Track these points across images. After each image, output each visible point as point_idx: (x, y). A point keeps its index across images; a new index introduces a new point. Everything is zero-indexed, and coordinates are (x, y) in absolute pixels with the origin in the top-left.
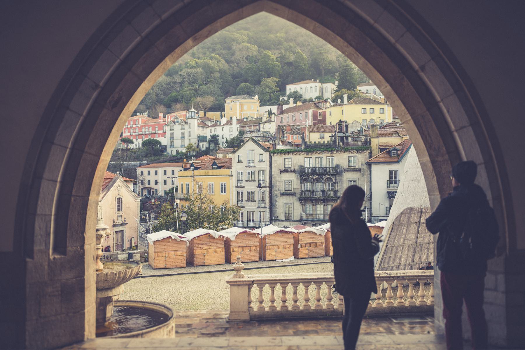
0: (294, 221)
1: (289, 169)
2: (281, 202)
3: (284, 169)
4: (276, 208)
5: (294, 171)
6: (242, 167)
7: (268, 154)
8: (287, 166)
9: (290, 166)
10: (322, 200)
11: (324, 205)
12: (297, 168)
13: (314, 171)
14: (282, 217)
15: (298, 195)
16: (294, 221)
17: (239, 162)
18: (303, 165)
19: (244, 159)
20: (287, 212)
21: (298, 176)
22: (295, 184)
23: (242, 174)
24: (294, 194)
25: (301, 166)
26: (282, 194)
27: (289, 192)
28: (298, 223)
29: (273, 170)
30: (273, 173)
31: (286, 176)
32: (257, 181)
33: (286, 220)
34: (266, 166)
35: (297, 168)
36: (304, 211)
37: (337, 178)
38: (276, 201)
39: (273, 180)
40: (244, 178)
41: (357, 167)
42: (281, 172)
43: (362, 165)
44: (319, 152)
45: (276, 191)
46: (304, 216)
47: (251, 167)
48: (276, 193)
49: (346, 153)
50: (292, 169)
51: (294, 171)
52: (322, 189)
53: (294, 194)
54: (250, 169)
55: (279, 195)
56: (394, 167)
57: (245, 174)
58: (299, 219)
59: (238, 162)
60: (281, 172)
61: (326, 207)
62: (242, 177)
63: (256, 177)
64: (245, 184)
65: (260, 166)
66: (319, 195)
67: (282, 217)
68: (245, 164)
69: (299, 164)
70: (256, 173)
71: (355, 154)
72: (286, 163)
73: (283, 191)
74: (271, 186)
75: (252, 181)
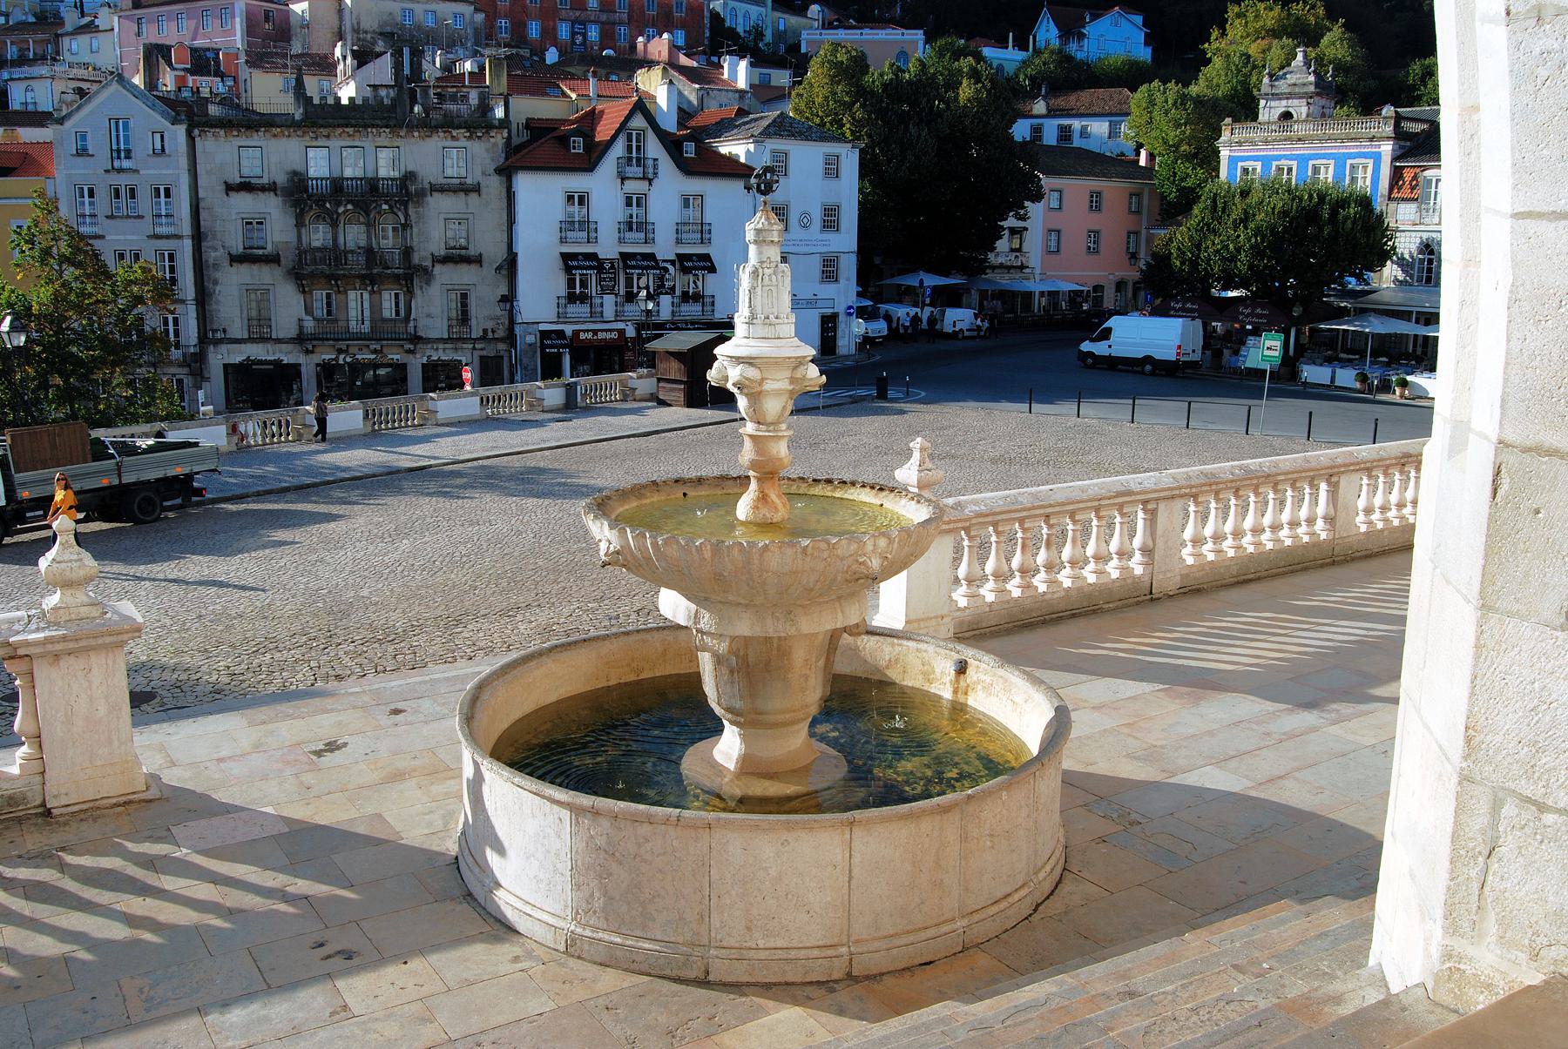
0: (279, 341)
1: (253, 181)
2: (232, 284)
3: (238, 180)
4: (218, 302)
5: (271, 188)
6: (92, 171)
7: (181, 130)
8: (246, 172)
9: (258, 172)
10: (362, 277)
11: (372, 292)
12: (281, 179)
13: (337, 186)
14: (237, 330)
15: (288, 259)
16: (279, 341)
17: (82, 152)
18: (300, 168)
19: (99, 144)
20: (254, 314)
21: (285, 202)
22: (279, 228)
23: (91, 194)
24: (273, 259)
25: (295, 173)
26: (236, 259)
27: (260, 252)
28: (290, 346)
29: (202, 181)
30: (201, 195)
31: (244, 203)
32: (149, 218)
33: (251, 340)
34: (175, 171)
35: (281, 179)
36: (309, 310)
37: (411, 211)
38: (216, 282)
39: (203, 215)
40: (103, 203)
41: (469, 181)
42: (230, 188)
43: (483, 173)
44: (350, 130)
45: (216, 250)
46: (309, 324)
47: (121, 170)
48: (213, 255)
49: (435, 138)
50: (265, 181)
51: (271, 188)
52: (363, 243)
53: (273, 259)
54: (122, 180)
55: (226, 263)
56: (577, 182)
57: (103, 195)
58: (293, 333)
59: (78, 154)
60: (230, 188)
61: (376, 296)
62: (91, 204)
63: (144, 202)
64: (104, 226)
65: (152, 173)
66: (358, 263)
67: (237, 330)
68: (103, 158)
69: (289, 168)
70: (144, 195)
71: (463, 142)
72: (244, 162)
73: (238, 247)
74: (198, 237)
75: (128, 217)
